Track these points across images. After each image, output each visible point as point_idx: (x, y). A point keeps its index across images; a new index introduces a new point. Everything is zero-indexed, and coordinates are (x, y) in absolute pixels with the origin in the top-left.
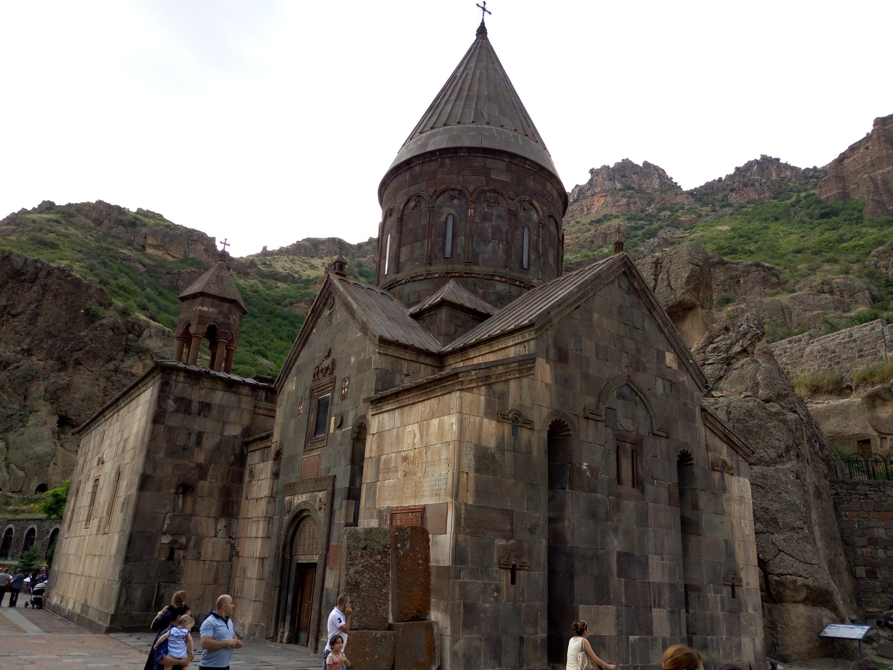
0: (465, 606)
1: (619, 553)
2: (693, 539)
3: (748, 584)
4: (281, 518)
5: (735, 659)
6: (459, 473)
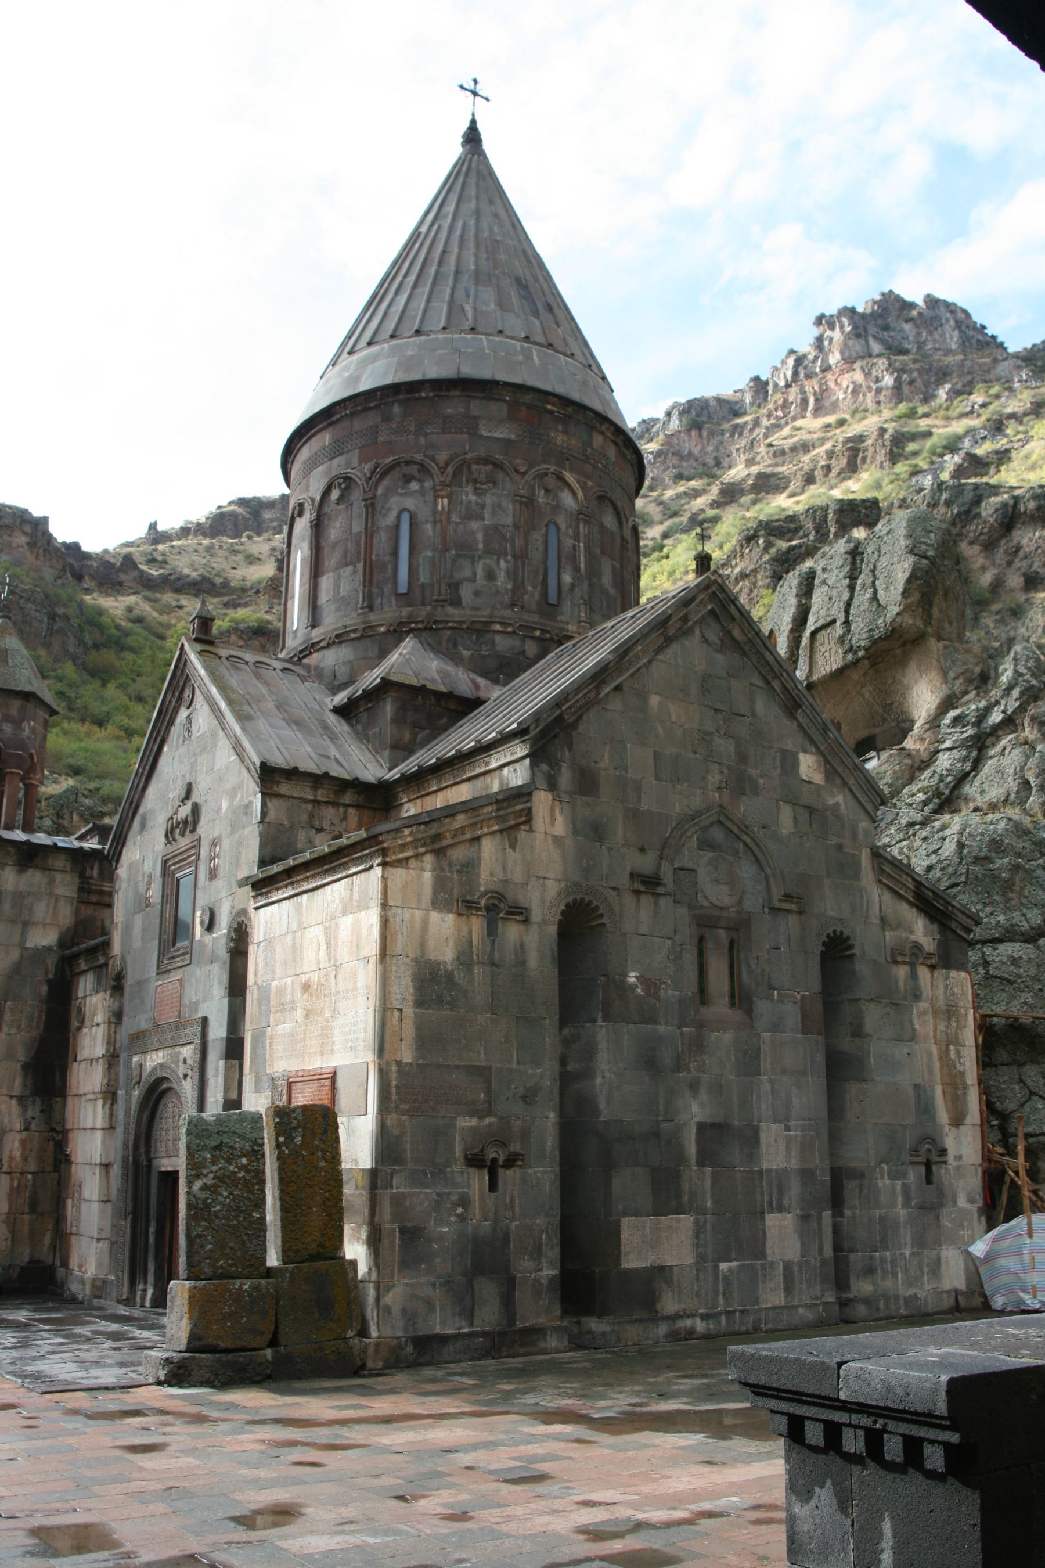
0: (403, 1231)
1: (701, 1126)
2: (853, 1089)
3: (958, 1158)
4: (128, 1094)
5: (927, 1287)
6: (385, 1009)
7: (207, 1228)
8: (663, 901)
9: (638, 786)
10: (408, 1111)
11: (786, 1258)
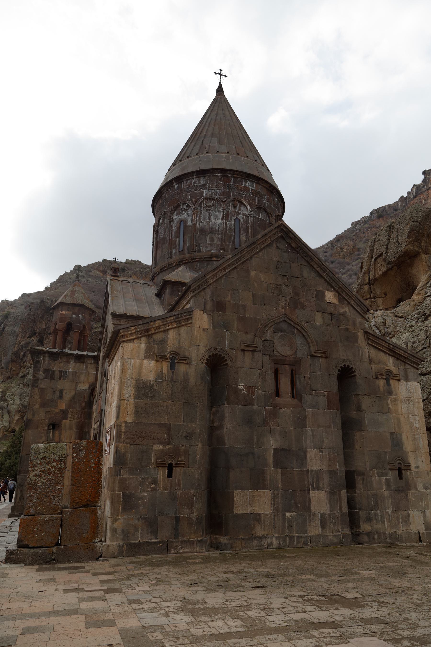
0: (124, 495)
1: (275, 450)
2: (358, 434)
5: (402, 529)
7: (34, 493)
8: (256, 354)
10: (130, 442)
11: (322, 512)
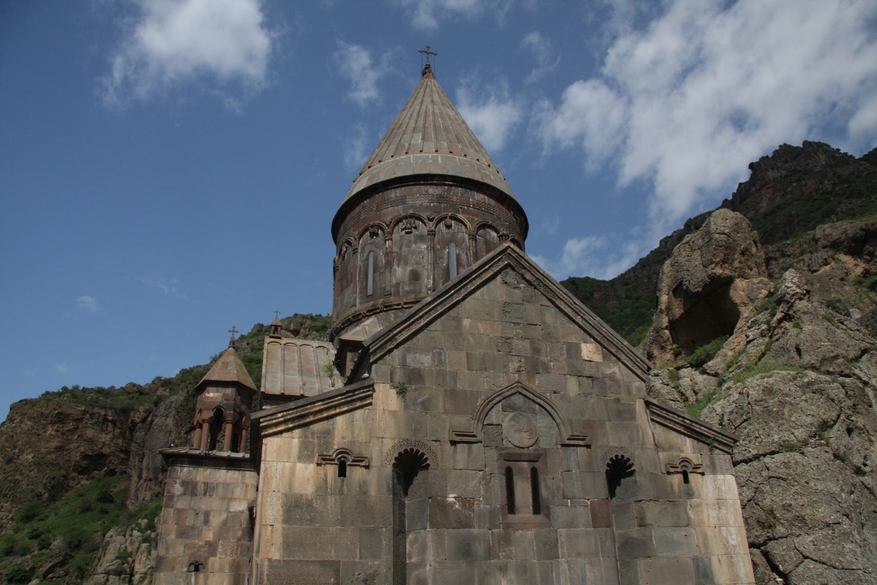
8: (474, 446)
9: (455, 376)
